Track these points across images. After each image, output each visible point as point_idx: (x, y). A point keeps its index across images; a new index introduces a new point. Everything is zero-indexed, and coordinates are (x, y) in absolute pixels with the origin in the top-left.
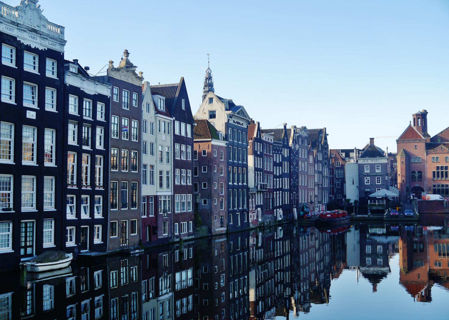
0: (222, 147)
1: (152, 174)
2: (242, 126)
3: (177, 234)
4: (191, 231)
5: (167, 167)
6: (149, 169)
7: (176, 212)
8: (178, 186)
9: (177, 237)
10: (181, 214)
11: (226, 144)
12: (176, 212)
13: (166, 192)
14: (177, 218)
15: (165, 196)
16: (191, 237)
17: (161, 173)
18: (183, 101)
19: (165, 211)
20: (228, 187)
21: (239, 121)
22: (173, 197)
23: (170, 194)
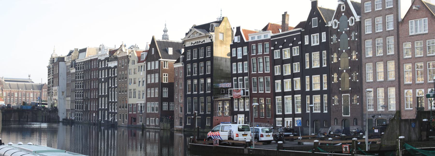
0: (180, 67)
1: (135, 93)
2: (203, 43)
3: (148, 124)
4: (157, 124)
5: (143, 88)
6: (132, 91)
7: (147, 112)
8: (149, 98)
9: (148, 126)
10: (150, 113)
11: (183, 64)
12: (147, 112)
13: (142, 101)
14: (149, 115)
15: (141, 104)
16: (157, 128)
17: (140, 92)
18: (153, 49)
19: (141, 111)
20: (186, 96)
21: (198, 41)
22: (146, 104)
23: (143, 102)
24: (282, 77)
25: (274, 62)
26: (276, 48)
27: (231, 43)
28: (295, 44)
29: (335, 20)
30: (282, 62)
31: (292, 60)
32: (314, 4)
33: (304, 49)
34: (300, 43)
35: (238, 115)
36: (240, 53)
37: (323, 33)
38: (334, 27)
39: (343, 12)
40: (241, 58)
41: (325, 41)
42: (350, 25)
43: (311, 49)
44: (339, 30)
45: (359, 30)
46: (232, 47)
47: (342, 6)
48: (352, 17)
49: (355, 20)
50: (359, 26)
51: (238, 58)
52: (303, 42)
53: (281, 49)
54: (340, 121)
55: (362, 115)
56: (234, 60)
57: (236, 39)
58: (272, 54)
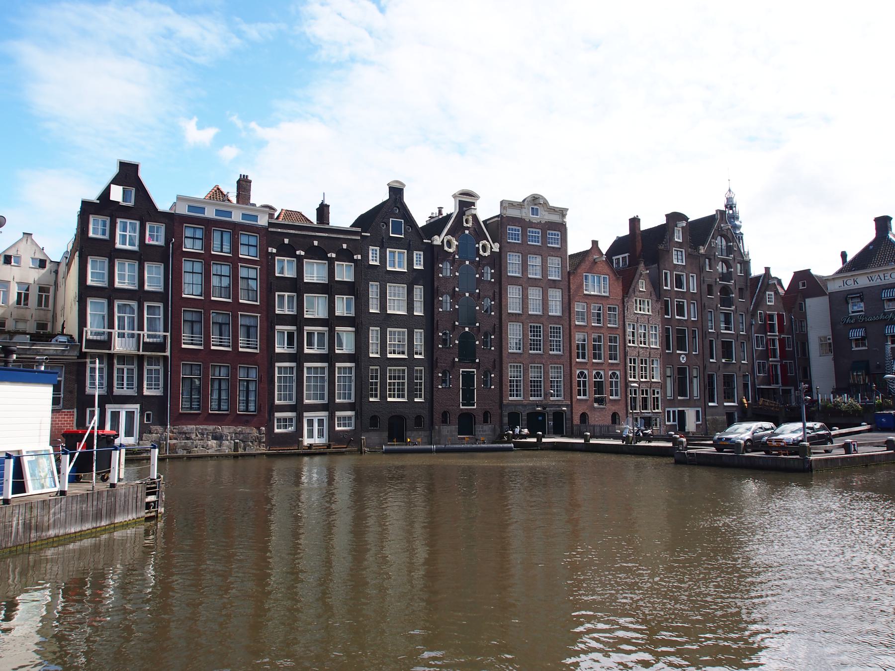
24: (298, 320)
25: (272, 285)
26: (287, 251)
27: (93, 196)
28: (345, 256)
29: (449, 237)
30: (297, 286)
31: (330, 289)
32: (396, 192)
33: (364, 271)
34: (359, 257)
35: (107, 406)
36: (126, 236)
37: (415, 253)
38: (446, 248)
39: (468, 228)
40: (136, 248)
41: (421, 267)
42: (481, 252)
43: (386, 277)
44: (457, 257)
45: (497, 267)
46: (87, 209)
47: (464, 218)
48: (485, 242)
49: (491, 248)
50: (497, 261)
51: (118, 245)
52: (366, 257)
53: (300, 259)
54: (454, 419)
55: (501, 405)
56: (85, 246)
57: (117, 194)
58: (267, 264)
